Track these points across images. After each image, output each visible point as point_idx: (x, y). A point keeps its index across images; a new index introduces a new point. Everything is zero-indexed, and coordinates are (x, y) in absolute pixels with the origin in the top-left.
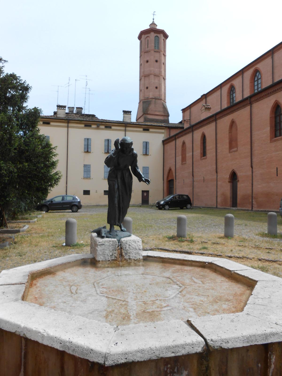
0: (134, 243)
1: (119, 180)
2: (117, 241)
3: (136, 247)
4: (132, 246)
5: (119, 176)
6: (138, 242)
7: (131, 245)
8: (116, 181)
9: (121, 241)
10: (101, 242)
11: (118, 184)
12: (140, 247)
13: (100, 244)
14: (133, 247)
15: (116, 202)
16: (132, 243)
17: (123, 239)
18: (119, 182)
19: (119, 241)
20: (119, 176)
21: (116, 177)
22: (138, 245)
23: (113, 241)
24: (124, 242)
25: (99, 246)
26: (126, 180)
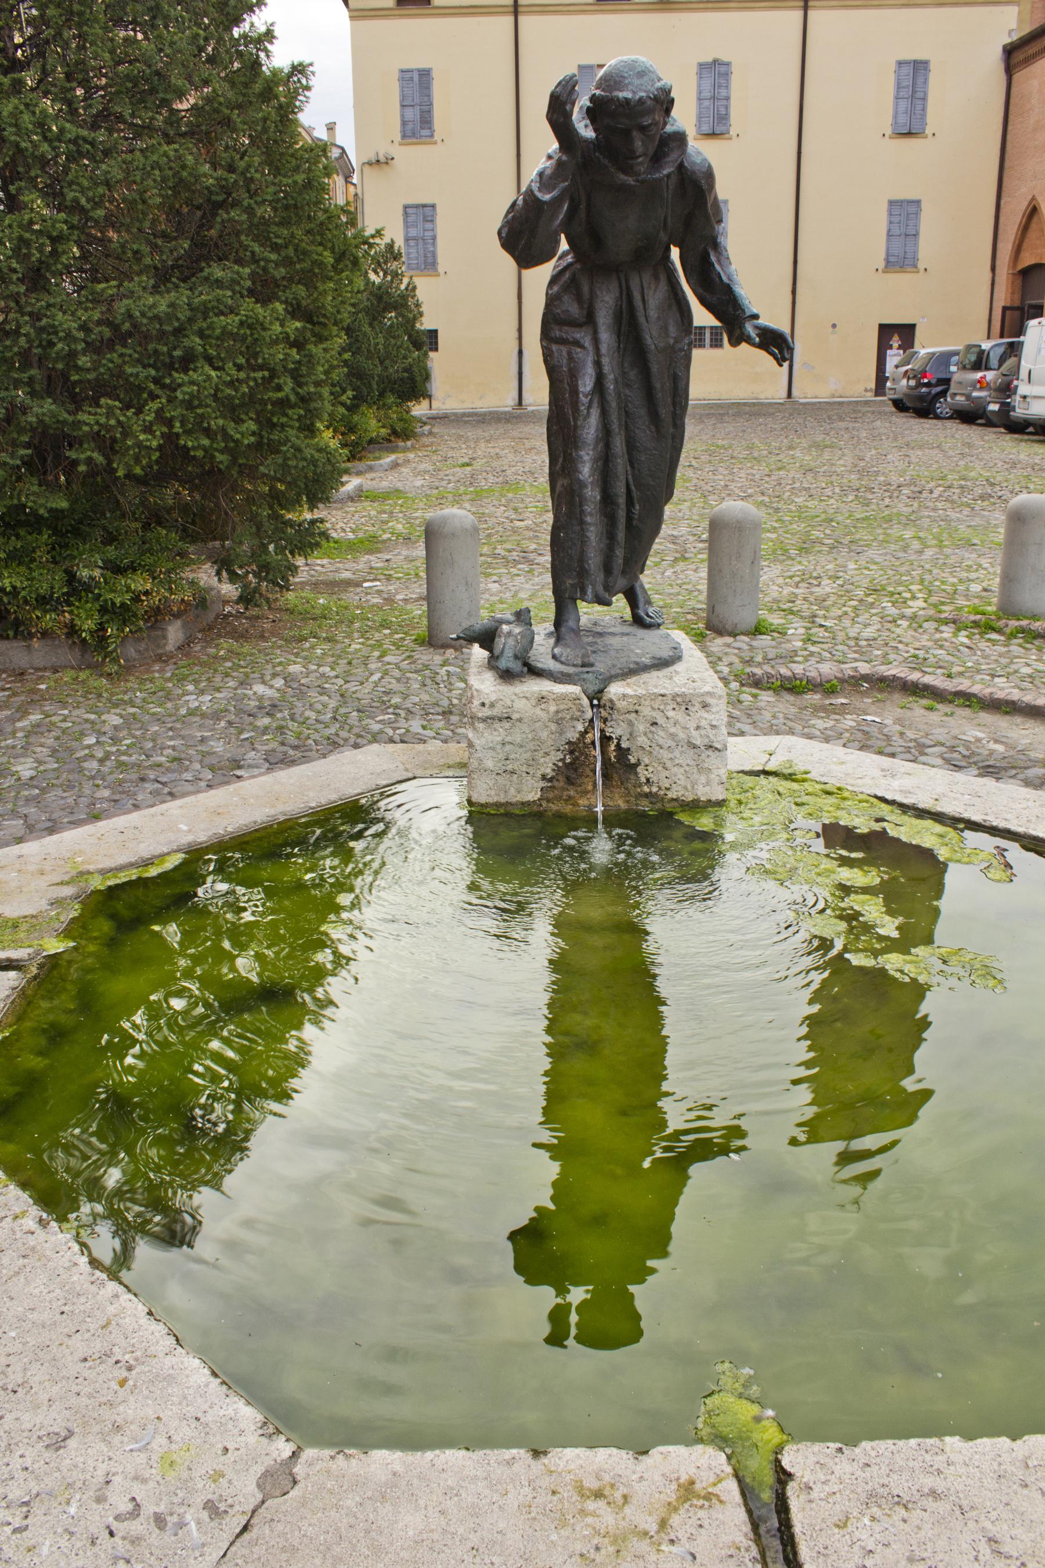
0: (679, 715)
1: (606, 337)
2: (585, 702)
3: (694, 733)
4: (664, 729)
5: (604, 318)
6: (705, 706)
7: (661, 721)
8: (587, 342)
9: (605, 697)
10: (492, 705)
11: (598, 364)
12: (711, 733)
13: (486, 712)
14: (673, 736)
15: (586, 471)
16: (671, 714)
17: (615, 690)
18: (604, 349)
19: (596, 697)
20: (604, 318)
21: (590, 320)
22: (703, 723)
23: (563, 697)
24: (621, 705)
25: (481, 726)
26: (652, 337)
